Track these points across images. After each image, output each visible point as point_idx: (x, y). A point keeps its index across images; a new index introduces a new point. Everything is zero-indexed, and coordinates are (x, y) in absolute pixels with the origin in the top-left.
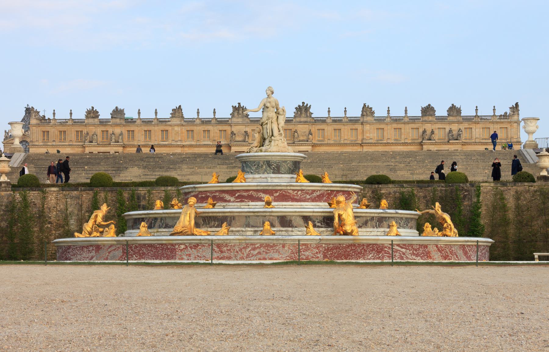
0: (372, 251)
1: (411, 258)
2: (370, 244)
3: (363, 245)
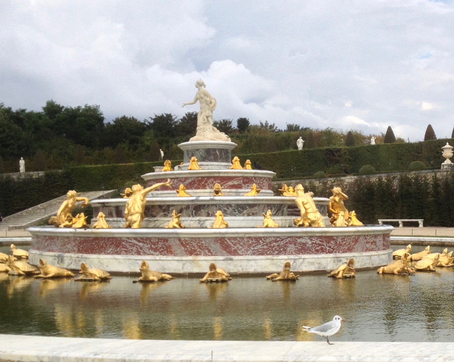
0: (111, 244)
1: (148, 253)
2: (110, 238)
3: (105, 238)
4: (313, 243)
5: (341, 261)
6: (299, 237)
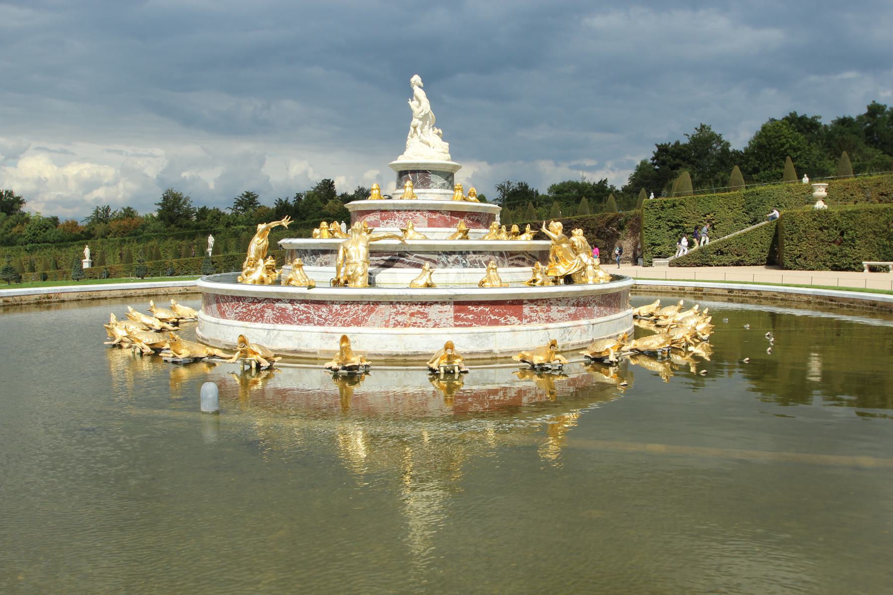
4: (294, 309)
5: (334, 338)
6: (278, 300)
